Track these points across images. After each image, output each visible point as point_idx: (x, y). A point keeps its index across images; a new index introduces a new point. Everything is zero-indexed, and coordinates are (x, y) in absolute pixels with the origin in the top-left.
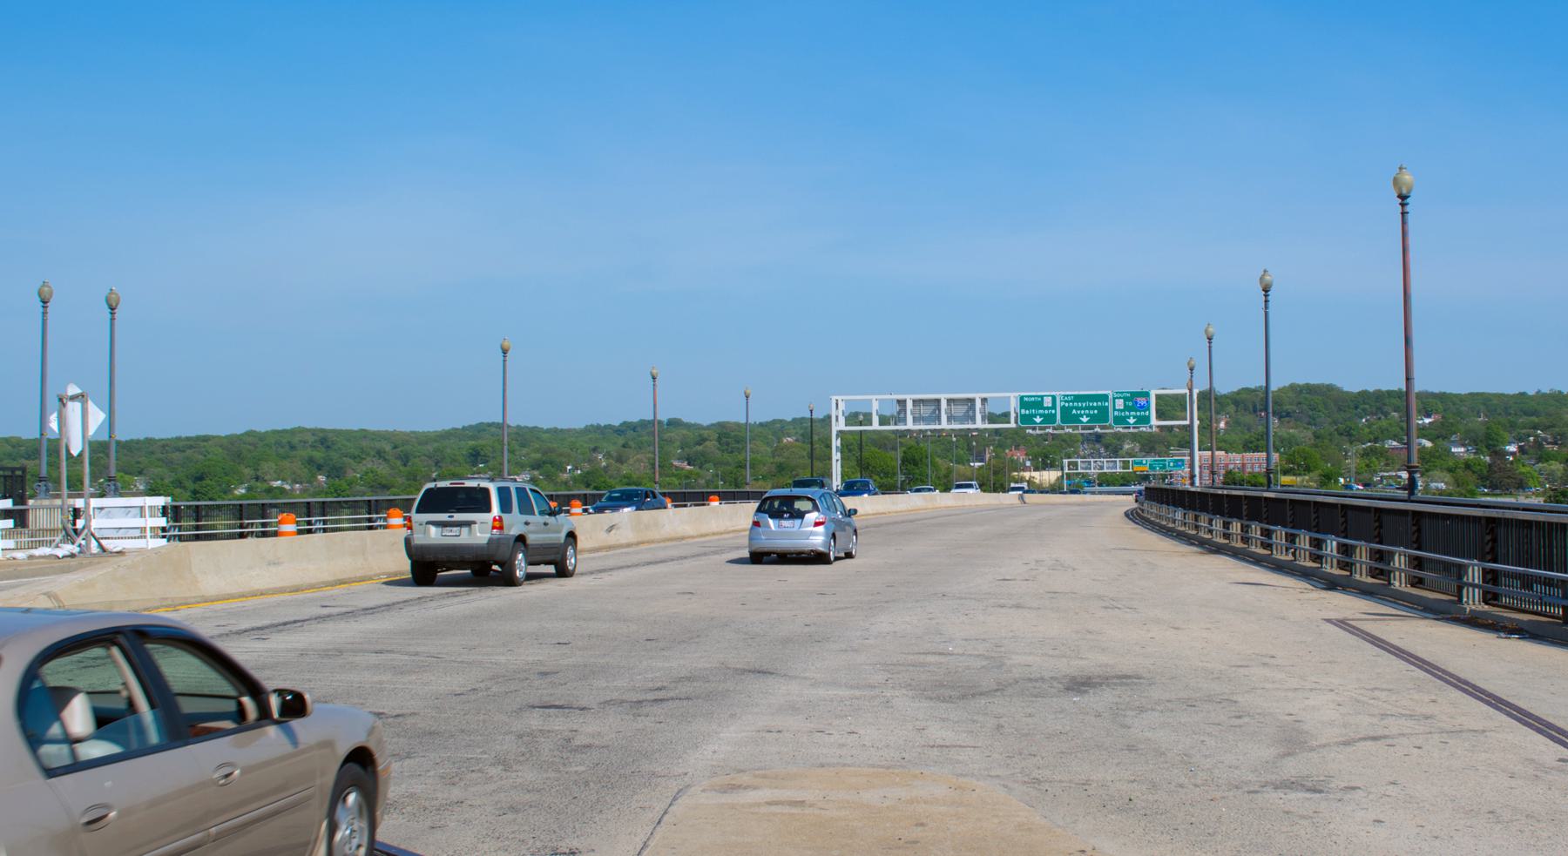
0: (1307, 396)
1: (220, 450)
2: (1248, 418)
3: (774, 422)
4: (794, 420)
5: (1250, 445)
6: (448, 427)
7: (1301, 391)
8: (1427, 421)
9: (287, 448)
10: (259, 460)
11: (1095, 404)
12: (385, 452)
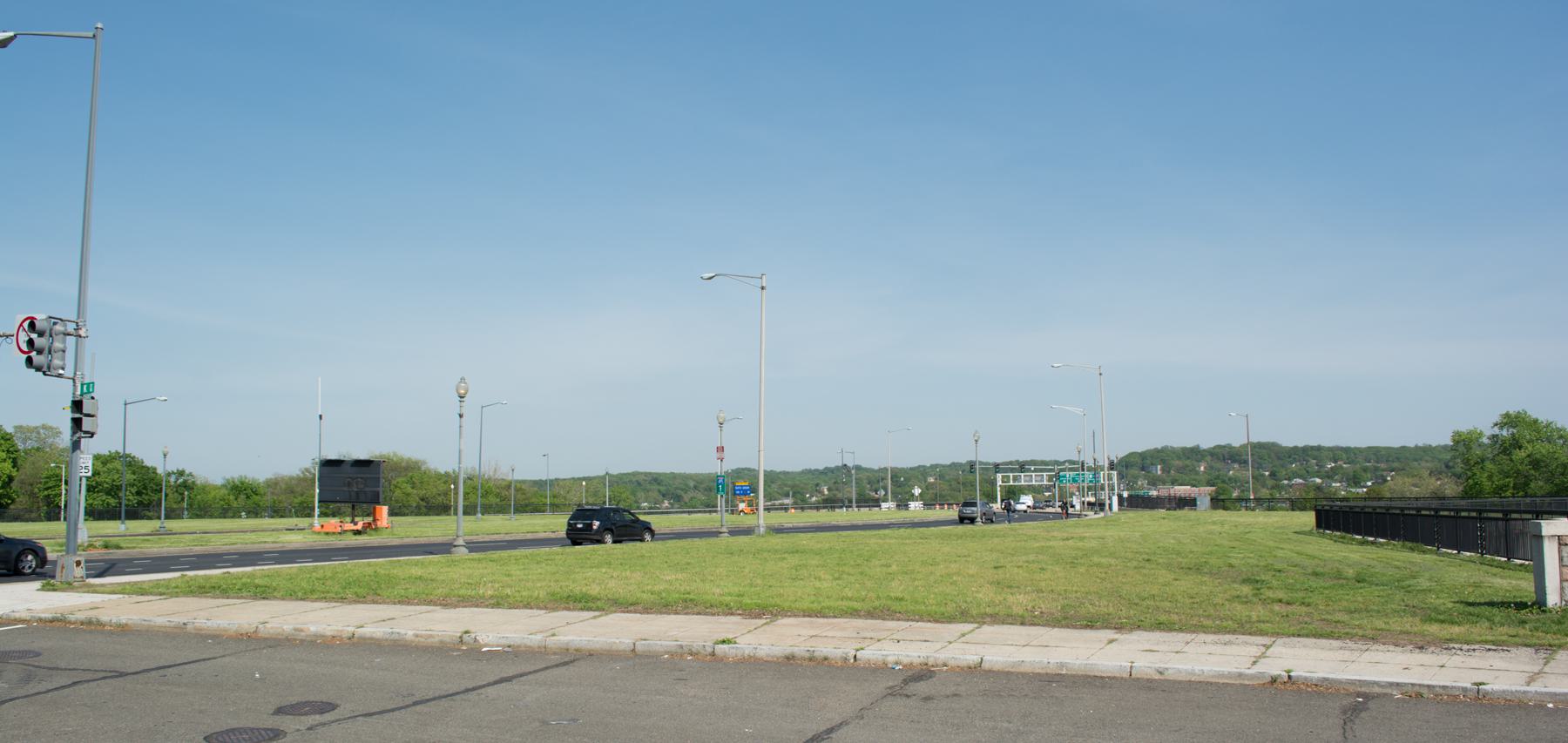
2: (1219, 465)
3: (919, 466)
4: (932, 466)
7: (1255, 447)
9: (636, 484)
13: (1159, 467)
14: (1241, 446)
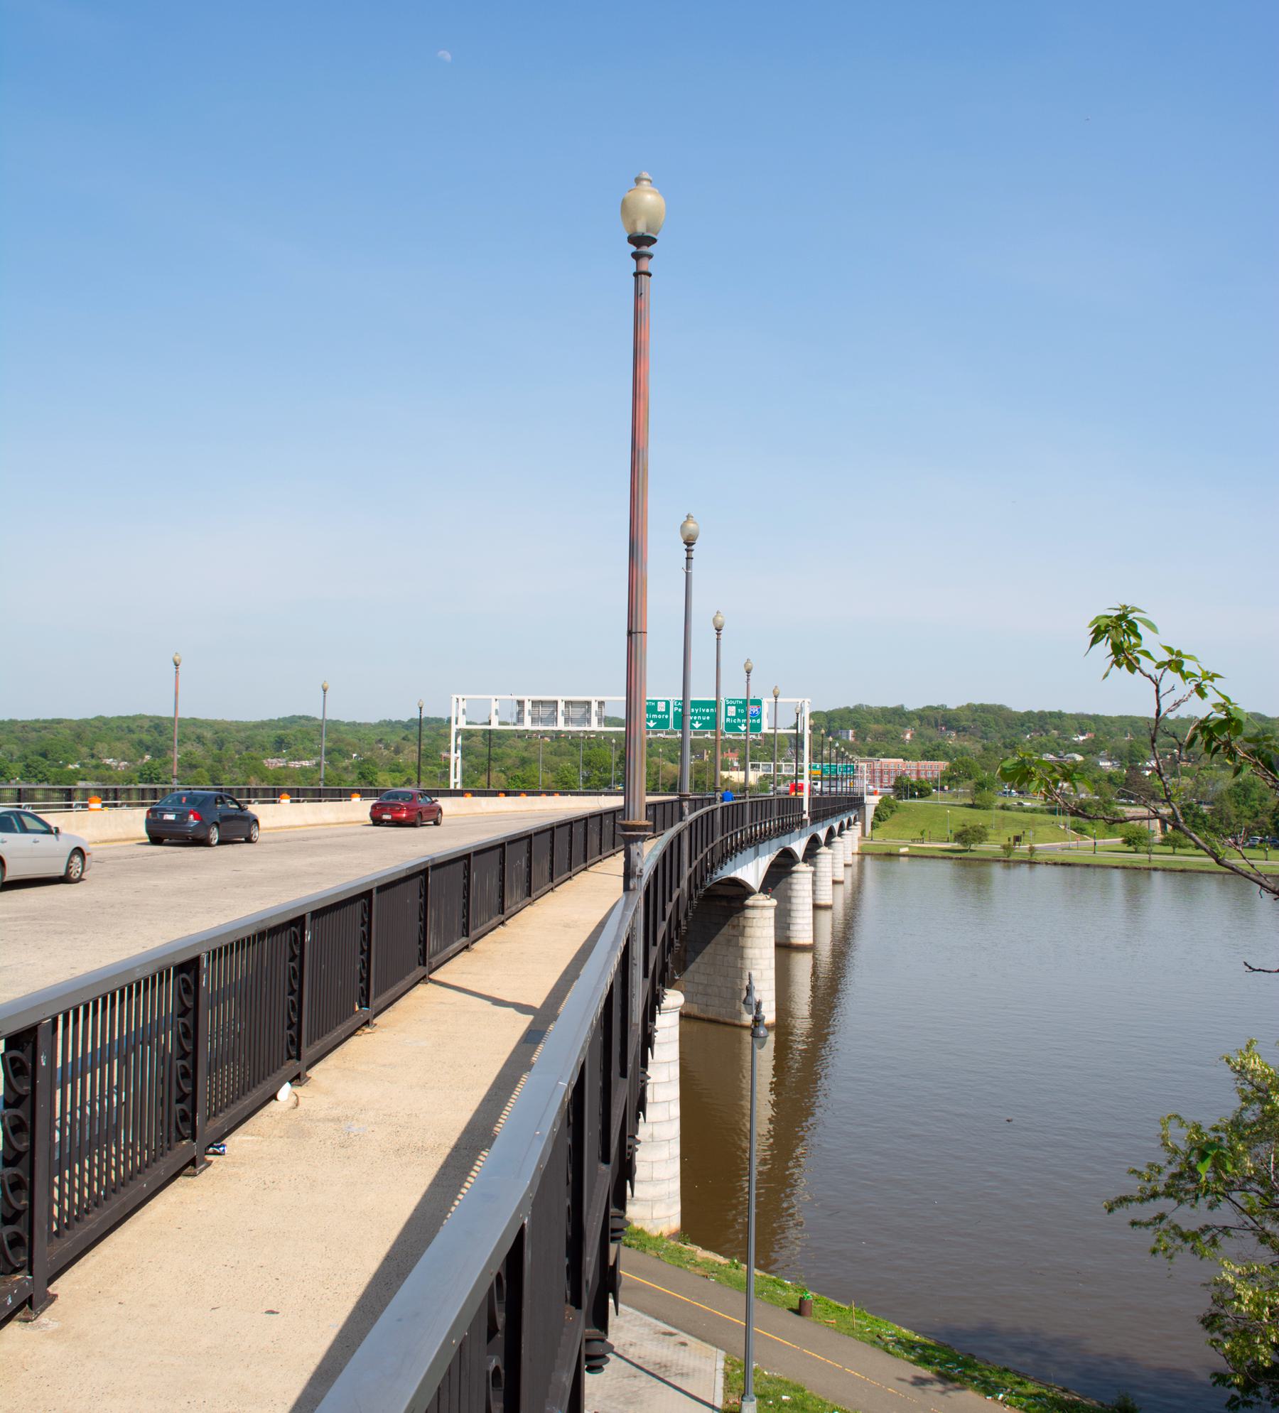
0: (982, 714)
1: (69, 732)
2: (930, 732)
5: (928, 754)
6: (266, 718)
7: (976, 711)
8: (1082, 738)
10: (97, 741)
11: (708, 711)
12: (203, 737)
13: (851, 732)
14: (958, 709)
